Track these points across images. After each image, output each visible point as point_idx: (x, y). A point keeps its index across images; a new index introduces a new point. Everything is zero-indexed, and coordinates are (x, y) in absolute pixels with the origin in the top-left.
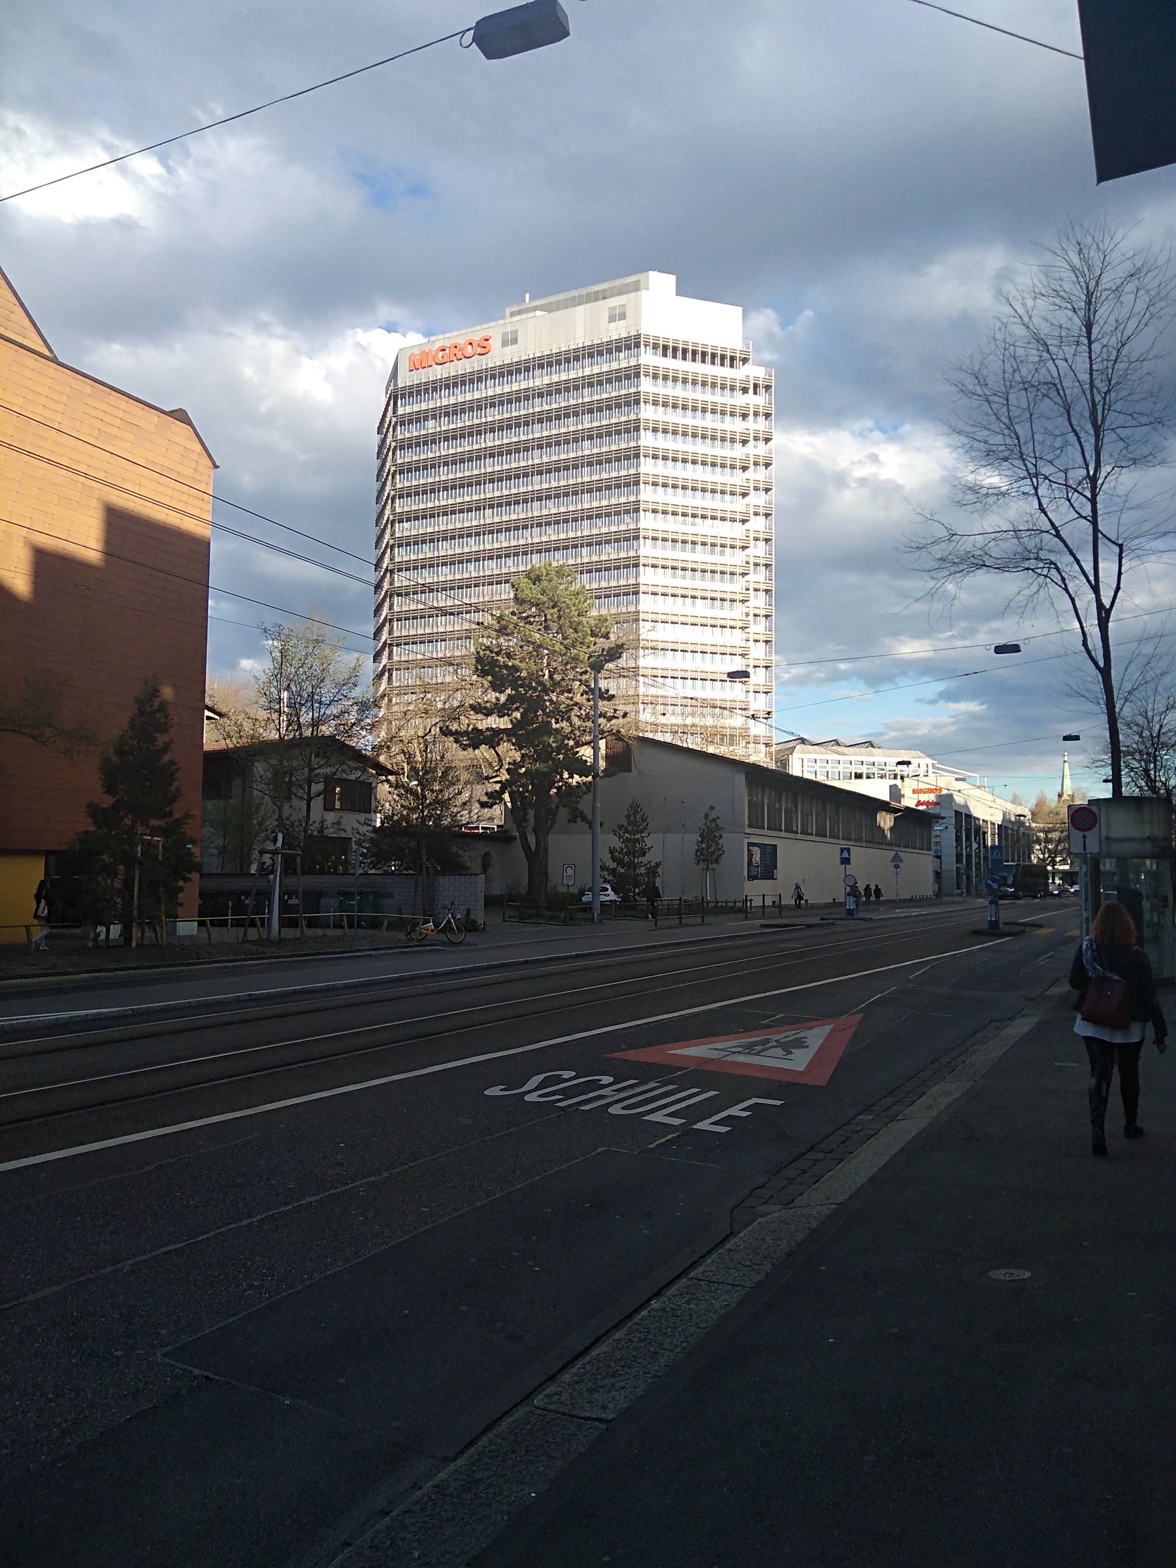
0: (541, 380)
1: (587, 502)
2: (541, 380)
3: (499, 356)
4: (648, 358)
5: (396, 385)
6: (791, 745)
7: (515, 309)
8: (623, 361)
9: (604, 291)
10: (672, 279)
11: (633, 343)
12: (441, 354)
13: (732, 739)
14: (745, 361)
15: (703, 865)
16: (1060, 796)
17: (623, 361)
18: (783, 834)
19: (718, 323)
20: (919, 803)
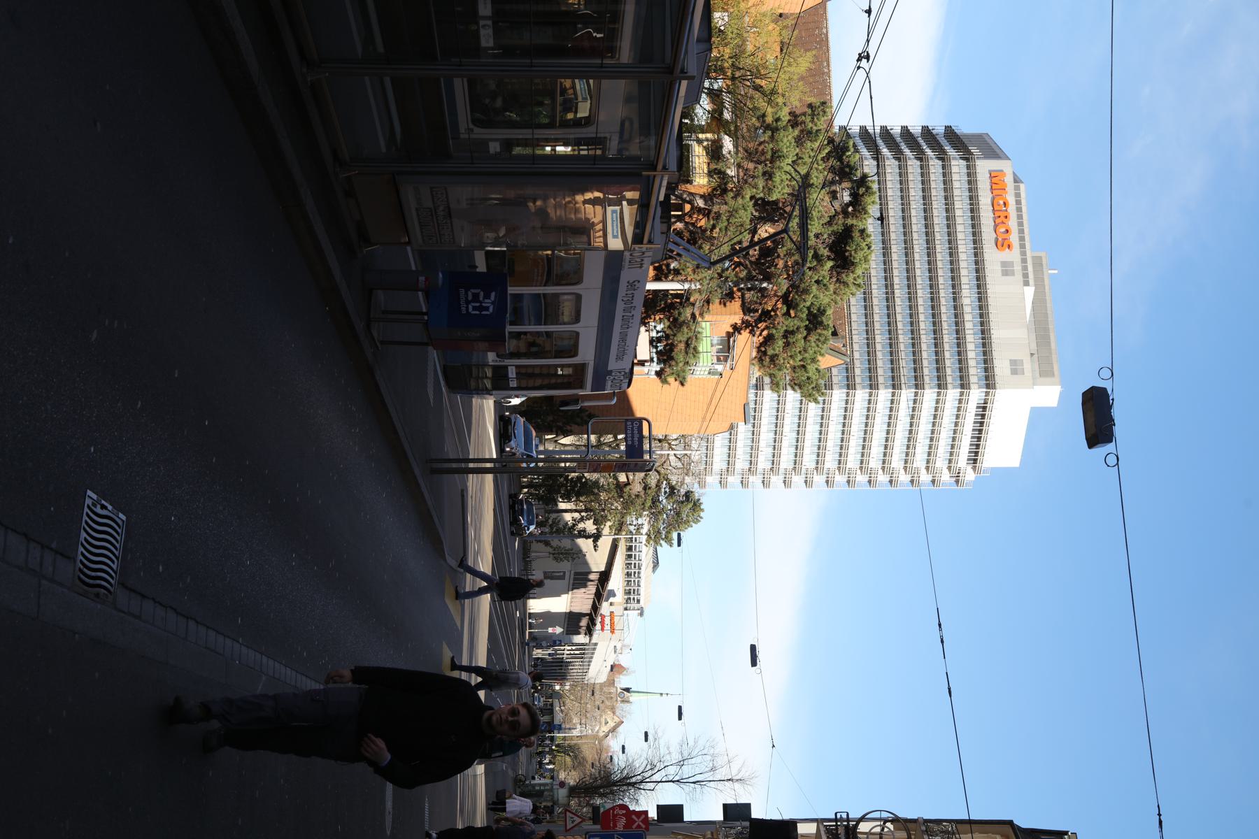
3: (992, 257)
4: (976, 395)
8: (975, 371)
11: (989, 382)
17: (975, 371)
20: (603, 617)
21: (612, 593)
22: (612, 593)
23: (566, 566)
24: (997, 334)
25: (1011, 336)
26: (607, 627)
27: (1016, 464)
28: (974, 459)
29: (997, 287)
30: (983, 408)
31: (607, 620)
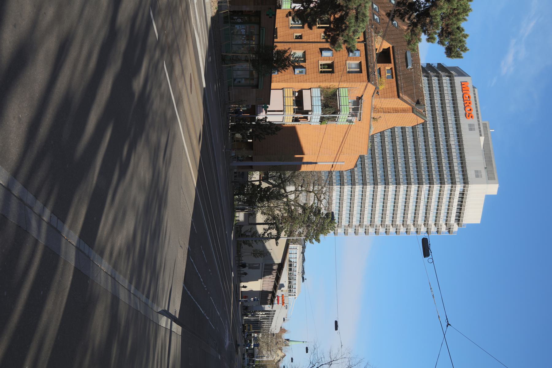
0: (453, 141)
2: (453, 141)
3: (464, 122)
8: (458, 176)
11: (465, 181)
12: (467, 96)
17: (458, 176)
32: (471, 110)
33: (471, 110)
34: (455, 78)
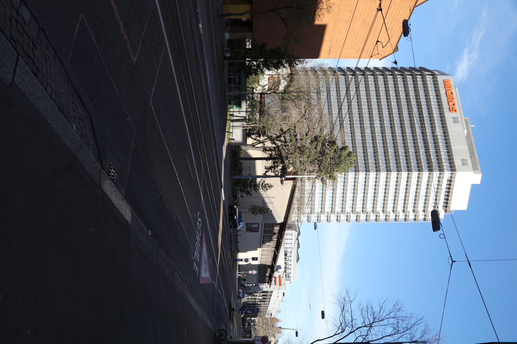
0: (439, 132)
1: (391, 151)
2: (439, 132)
3: (449, 116)
4: (447, 175)
5: (438, 75)
6: (298, 230)
7: (468, 122)
8: (446, 164)
9: (474, 156)
10: (478, 182)
11: (452, 168)
12: (450, 93)
13: (299, 209)
14: (446, 211)
15: (251, 208)
16: (280, 328)
17: (446, 164)
18: (263, 234)
19: (460, 201)
20: (275, 278)
21: (279, 267)
22: (279, 267)
23: (258, 219)
24: (454, 148)
25: (460, 149)
26: (278, 282)
27: (465, 209)
28: (446, 206)
29: (452, 128)
30: (450, 181)
31: (278, 279)
32: (454, 104)
33: (454, 104)
34: (438, 76)
